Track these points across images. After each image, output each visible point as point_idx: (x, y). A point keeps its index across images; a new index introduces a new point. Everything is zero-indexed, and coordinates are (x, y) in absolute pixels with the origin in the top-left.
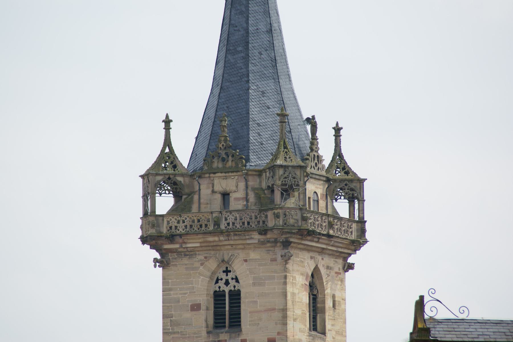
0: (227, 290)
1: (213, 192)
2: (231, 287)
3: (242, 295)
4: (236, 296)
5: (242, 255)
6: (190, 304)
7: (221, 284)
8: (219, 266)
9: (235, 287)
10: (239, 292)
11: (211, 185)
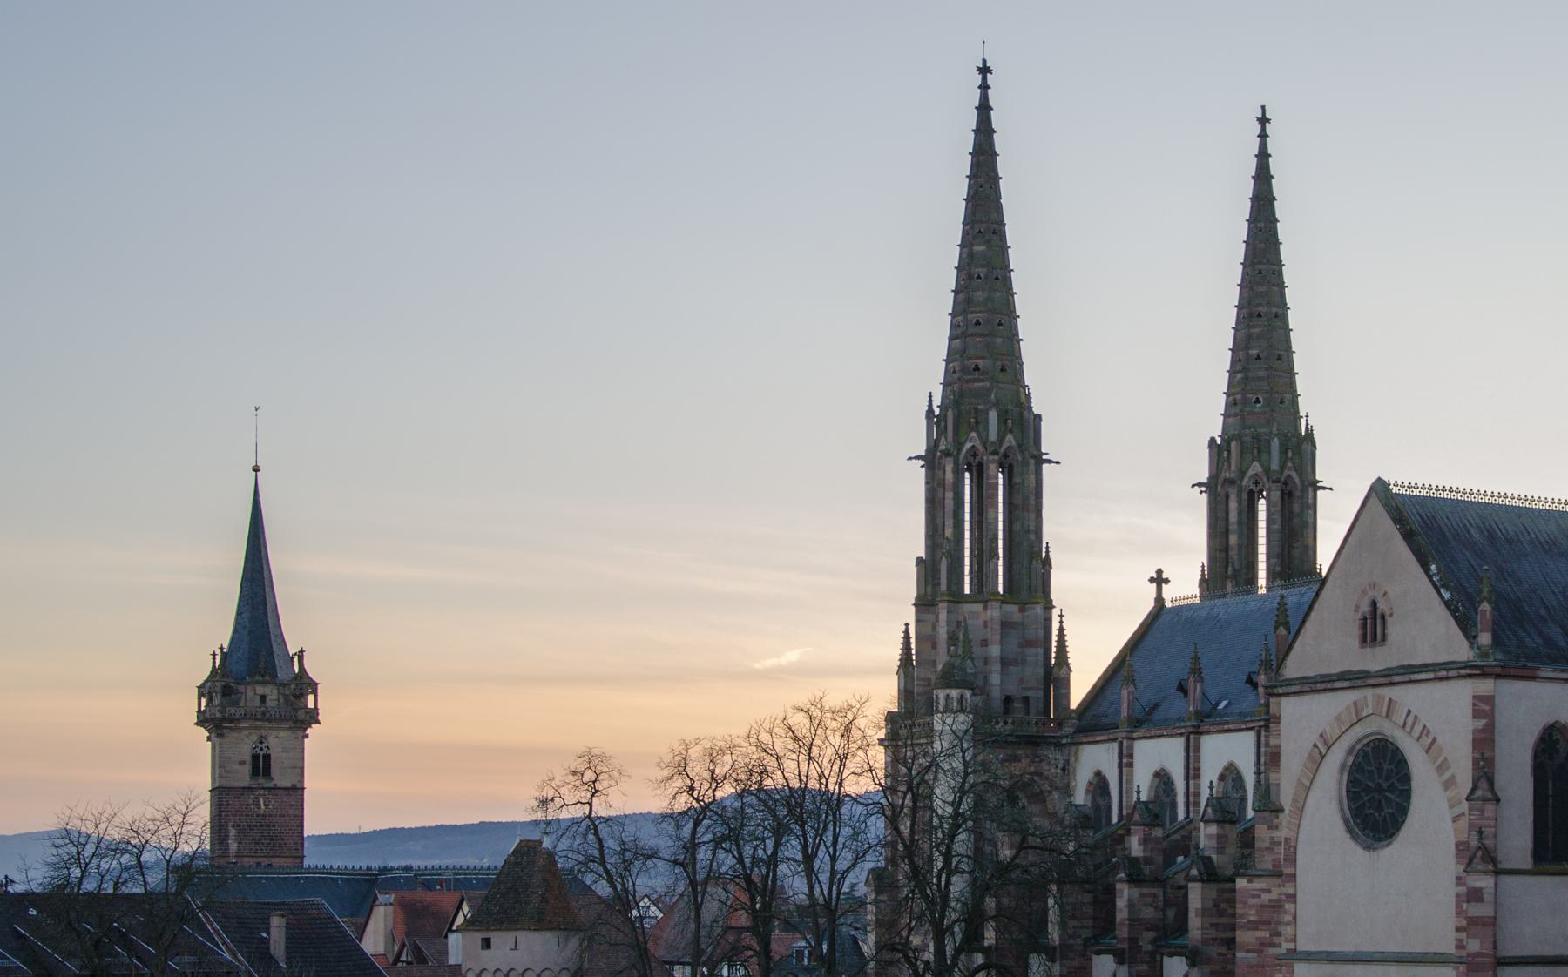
0: (261, 753)
1: (255, 694)
2: (264, 752)
3: (272, 757)
4: (267, 757)
5: (274, 733)
7: (258, 750)
10: (270, 755)
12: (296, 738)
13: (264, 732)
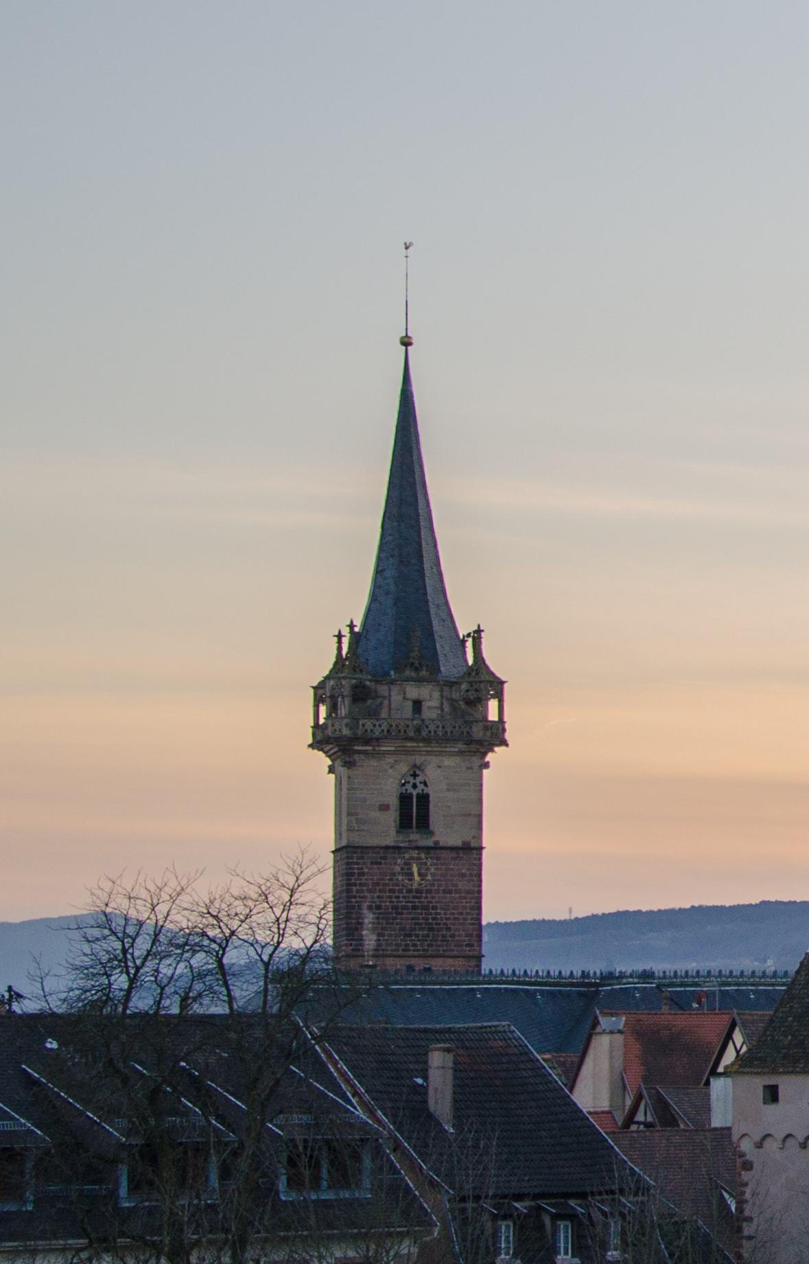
0: (415, 793)
1: (404, 698)
2: (419, 790)
3: (431, 799)
4: (424, 799)
5: (435, 760)
6: (377, 804)
7: (409, 787)
8: (409, 771)
9: (423, 790)
11: (402, 692)
12: (471, 768)
13: (418, 760)
